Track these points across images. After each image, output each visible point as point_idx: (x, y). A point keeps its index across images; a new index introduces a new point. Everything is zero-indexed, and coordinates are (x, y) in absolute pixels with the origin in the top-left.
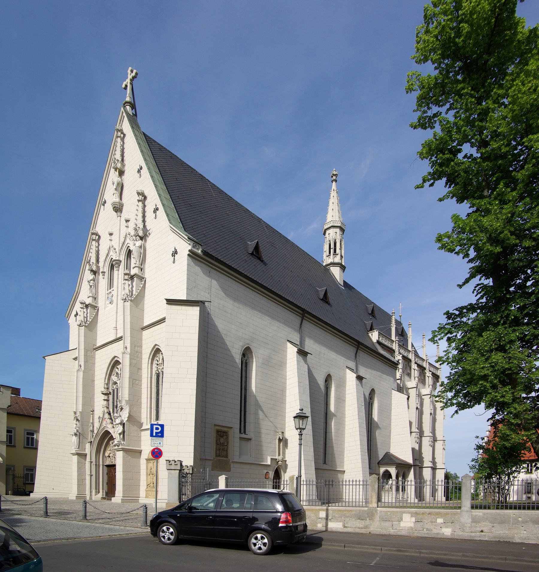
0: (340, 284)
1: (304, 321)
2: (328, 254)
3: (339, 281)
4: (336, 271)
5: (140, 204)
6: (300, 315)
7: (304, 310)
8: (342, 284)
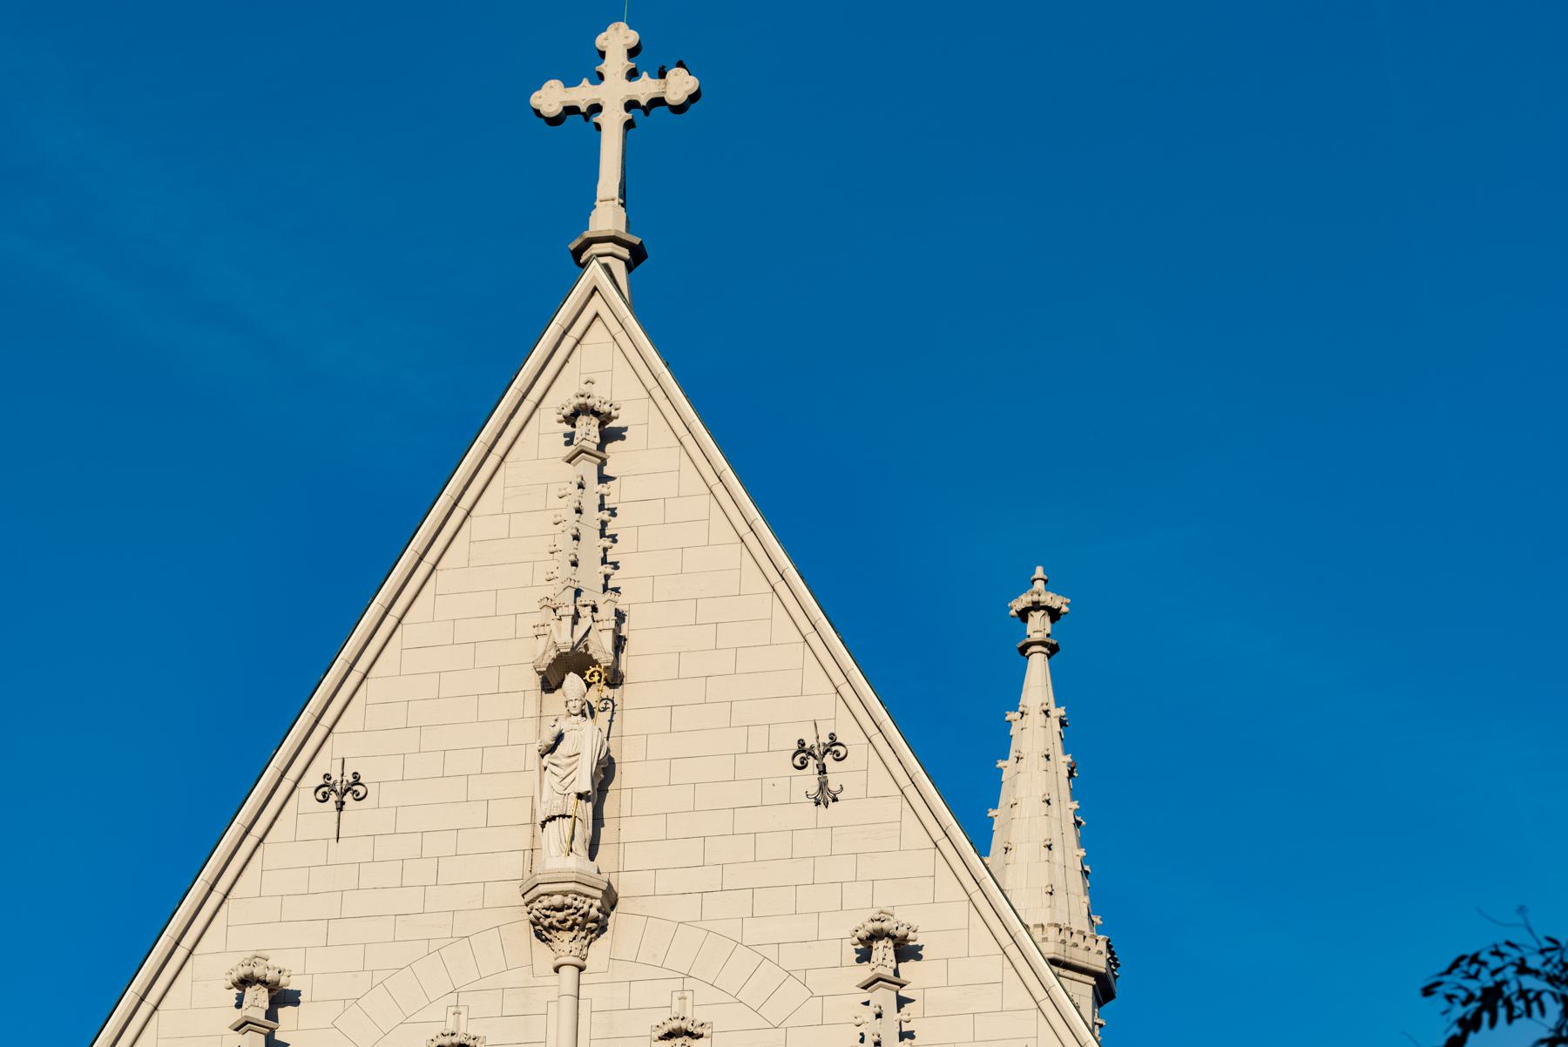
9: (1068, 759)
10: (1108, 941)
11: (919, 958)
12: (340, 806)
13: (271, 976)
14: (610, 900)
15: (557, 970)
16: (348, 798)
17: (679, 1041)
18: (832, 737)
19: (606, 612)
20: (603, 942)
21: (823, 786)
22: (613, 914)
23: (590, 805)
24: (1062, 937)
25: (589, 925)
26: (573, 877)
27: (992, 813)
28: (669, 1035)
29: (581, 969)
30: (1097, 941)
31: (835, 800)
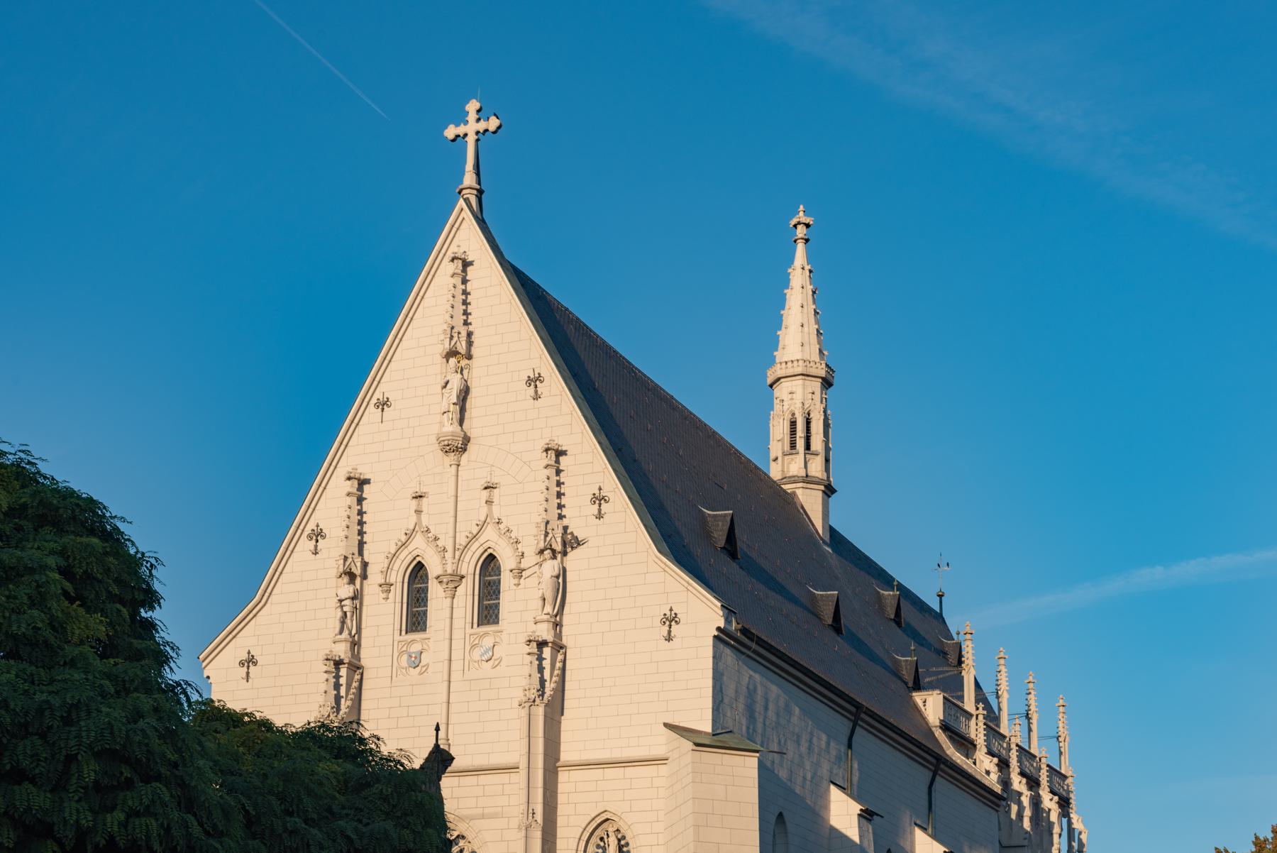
0: (824, 542)
1: (858, 729)
3: (821, 532)
4: (811, 501)
6: (848, 715)
7: (858, 706)
8: (827, 539)
9: (812, 287)
11: (566, 455)
12: (383, 409)
13: (357, 476)
14: (467, 440)
15: (451, 466)
16: (385, 407)
17: (488, 490)
18: (539, 374)
19: (464, 334)
20: (465, 456)
21: (536, 392)
22: (469, 444)
23: (458, 407)
24: (805, 364)
26: (450, 434)
27: (782, 312)
28: (486, 488)
29: (458, 465)
31: (540, 397)
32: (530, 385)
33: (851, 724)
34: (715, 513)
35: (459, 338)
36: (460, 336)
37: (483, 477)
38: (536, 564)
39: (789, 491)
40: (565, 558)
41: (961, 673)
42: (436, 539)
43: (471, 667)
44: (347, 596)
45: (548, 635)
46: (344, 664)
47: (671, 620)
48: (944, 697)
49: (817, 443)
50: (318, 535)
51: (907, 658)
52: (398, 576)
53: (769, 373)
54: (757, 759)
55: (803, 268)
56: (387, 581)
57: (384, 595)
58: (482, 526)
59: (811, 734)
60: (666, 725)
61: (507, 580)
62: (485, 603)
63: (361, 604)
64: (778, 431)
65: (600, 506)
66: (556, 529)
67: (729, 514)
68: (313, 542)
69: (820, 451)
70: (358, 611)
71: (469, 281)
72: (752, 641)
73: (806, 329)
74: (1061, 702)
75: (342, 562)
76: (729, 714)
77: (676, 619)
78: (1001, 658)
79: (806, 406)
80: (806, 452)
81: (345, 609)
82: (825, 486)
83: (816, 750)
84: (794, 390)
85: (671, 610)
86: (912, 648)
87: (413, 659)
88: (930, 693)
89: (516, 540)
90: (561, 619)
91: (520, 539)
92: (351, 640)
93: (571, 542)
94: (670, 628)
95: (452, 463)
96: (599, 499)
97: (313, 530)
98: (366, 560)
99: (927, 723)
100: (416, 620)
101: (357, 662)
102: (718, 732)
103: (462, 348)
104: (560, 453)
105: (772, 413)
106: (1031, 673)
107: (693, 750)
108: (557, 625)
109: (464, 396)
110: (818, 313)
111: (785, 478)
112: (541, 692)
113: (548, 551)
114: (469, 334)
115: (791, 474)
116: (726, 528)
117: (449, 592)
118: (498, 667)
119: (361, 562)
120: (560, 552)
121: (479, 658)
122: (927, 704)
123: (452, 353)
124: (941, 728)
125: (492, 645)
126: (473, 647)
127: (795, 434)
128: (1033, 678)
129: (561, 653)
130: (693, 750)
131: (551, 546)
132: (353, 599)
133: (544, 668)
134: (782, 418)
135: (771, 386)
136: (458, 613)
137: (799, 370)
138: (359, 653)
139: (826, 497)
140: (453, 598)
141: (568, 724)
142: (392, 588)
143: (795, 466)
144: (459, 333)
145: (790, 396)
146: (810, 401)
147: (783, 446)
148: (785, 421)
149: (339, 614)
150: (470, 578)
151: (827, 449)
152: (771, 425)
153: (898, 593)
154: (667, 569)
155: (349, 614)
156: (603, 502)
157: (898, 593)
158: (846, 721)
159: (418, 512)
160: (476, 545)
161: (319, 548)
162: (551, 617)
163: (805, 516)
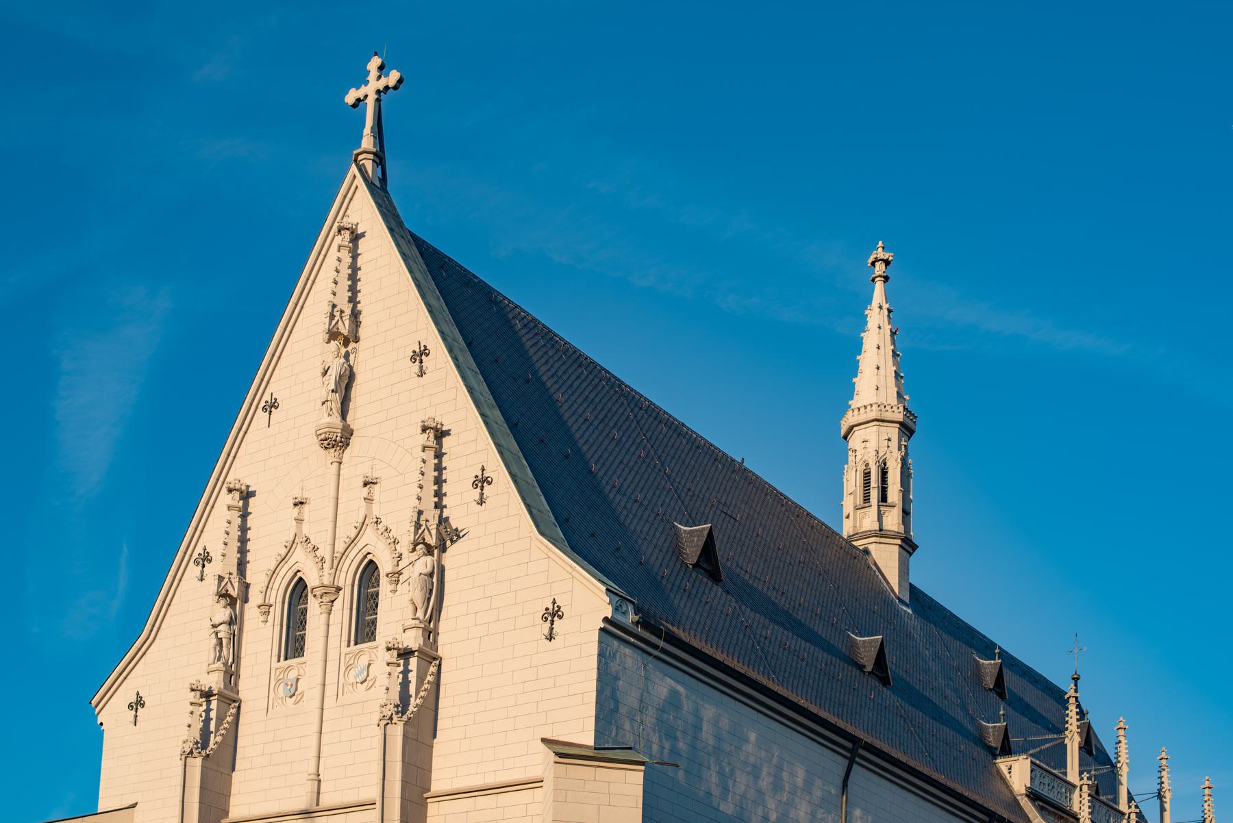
0: (901, 601)
2: (860, 501)
3: (896, 590)
4: (886, 558)
5: (430, 454)
8: (906, 598)
9: (890, 327)
10: (904, 407)
13: (237, 486)
15: (332, 464)
16: (273, 409)
17: (368, 486)
20: (348, 451)
25: (340, 444)
29: (340, 463)
30: (898, 408)
32: (415, 360)
33: (847, 762)
34: (692, 528)
35: (341, 317)
36: (343, 315)
37: (364, 471)
38: (410, 564)
39: (861, 548)
40: (444, 555)
41: (1064, 742)
42: (315, 549)
43: (346, 691)
44: (221, 621)
45: (415, 643)
46: (215, 695)
47: (553, 614)
48: (1032, 762)
49: (894, 494)
50: (206, 558)
51: (995, 724)
52: (277, 596)
53: (842, 422)
54: (642, 773)
55: (880, 307)
56: (267, 602)
57: (262, 618)
58: (360, 529)
59: (779, 768)
60: (544, 740)
61: (385, 586)
62: (367, 618)
63: (241, 630)
64: (852, 482)
65: (482, 490)
66: (431, 519)
67: (708, 527)
68: (200, 567)
69: (897, 502)
70: (236, 640)
71: (360, 254)
72: (660, 638)
73: (882, 370)
74: (1207, 784)
75: (216, 582)
76: (627, 726)
77: (560, 613)
78: (1120, 728)
79: (881, 454)
80: (880, 504)
81: (220, 635)
82: (902, 540)
83: (787, 787)
84: (867, 438)
85: (554, 602)
86: (1002, 712)
87: (289, 687)
88: (1016, 758)
89: (393, 540)
90: (436, 626)
91: (399, 538)
92: (224, 669)
93: (448, 535)
94: (552, 624)
95: (334, 460)
96: (482, 482)
97: (200, 554)
98: (248, 581)
99: (1011, 792)
100: (294, 646)
101: (236, 696)
102: (606, 746)
103: (344, 328)
104: (440, 434)
105: (846, 466)
106: (1164, 748)
107: (556, 762)
108: (430, 633)
109: (347, 384)
110: (899, 355)
111: (857, 534)
112: (400, 709)
113: (421, 546)
114: (355, 315)
115: (864, 529)
116: (702, 543)
117: (324, 607)
118: (373, 688)
119: (239, 582)
120: (436, 548)
121: (354, 681)
122: (1012, 770)
123: (333, 335)
124: (1027, 796)
125: (367, 664)
126: (349, 667)
127: (869, 486)
128: (1166, 755)
129: (433, 664)
130: (556, 762)
131: (424, 539)
132: (231, 622)
133: (410, 682)
134: (854, 469)
135: (845, 438)
136: (335, 631)
137: (873, 414)
138: (236, 684)
139: (905, 553)
140: (329, 614)
141: (443, 749)
142: (272, 609)
143: (868, 521)
144: (342, 312)
145: (863, 445)
146: (886, 448)
147: (855, 499)
148: (858, 473)
149: (214, 641)
150: (347, 592)
151: (906, 500)
152: (845, 480)
153: (1000, 661)
154: (550, 554)
155: (224, 641)
156: (485, 484)
157: (1000, 661)
158: (839, 759)
159: (299, 520)
160: (356, 550)
161: (205, 573)
162: (420, 622)
163: (877, 573)
